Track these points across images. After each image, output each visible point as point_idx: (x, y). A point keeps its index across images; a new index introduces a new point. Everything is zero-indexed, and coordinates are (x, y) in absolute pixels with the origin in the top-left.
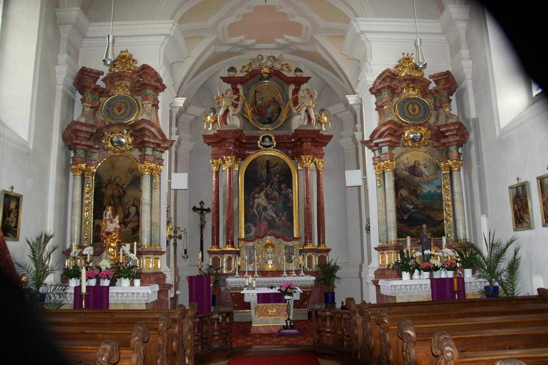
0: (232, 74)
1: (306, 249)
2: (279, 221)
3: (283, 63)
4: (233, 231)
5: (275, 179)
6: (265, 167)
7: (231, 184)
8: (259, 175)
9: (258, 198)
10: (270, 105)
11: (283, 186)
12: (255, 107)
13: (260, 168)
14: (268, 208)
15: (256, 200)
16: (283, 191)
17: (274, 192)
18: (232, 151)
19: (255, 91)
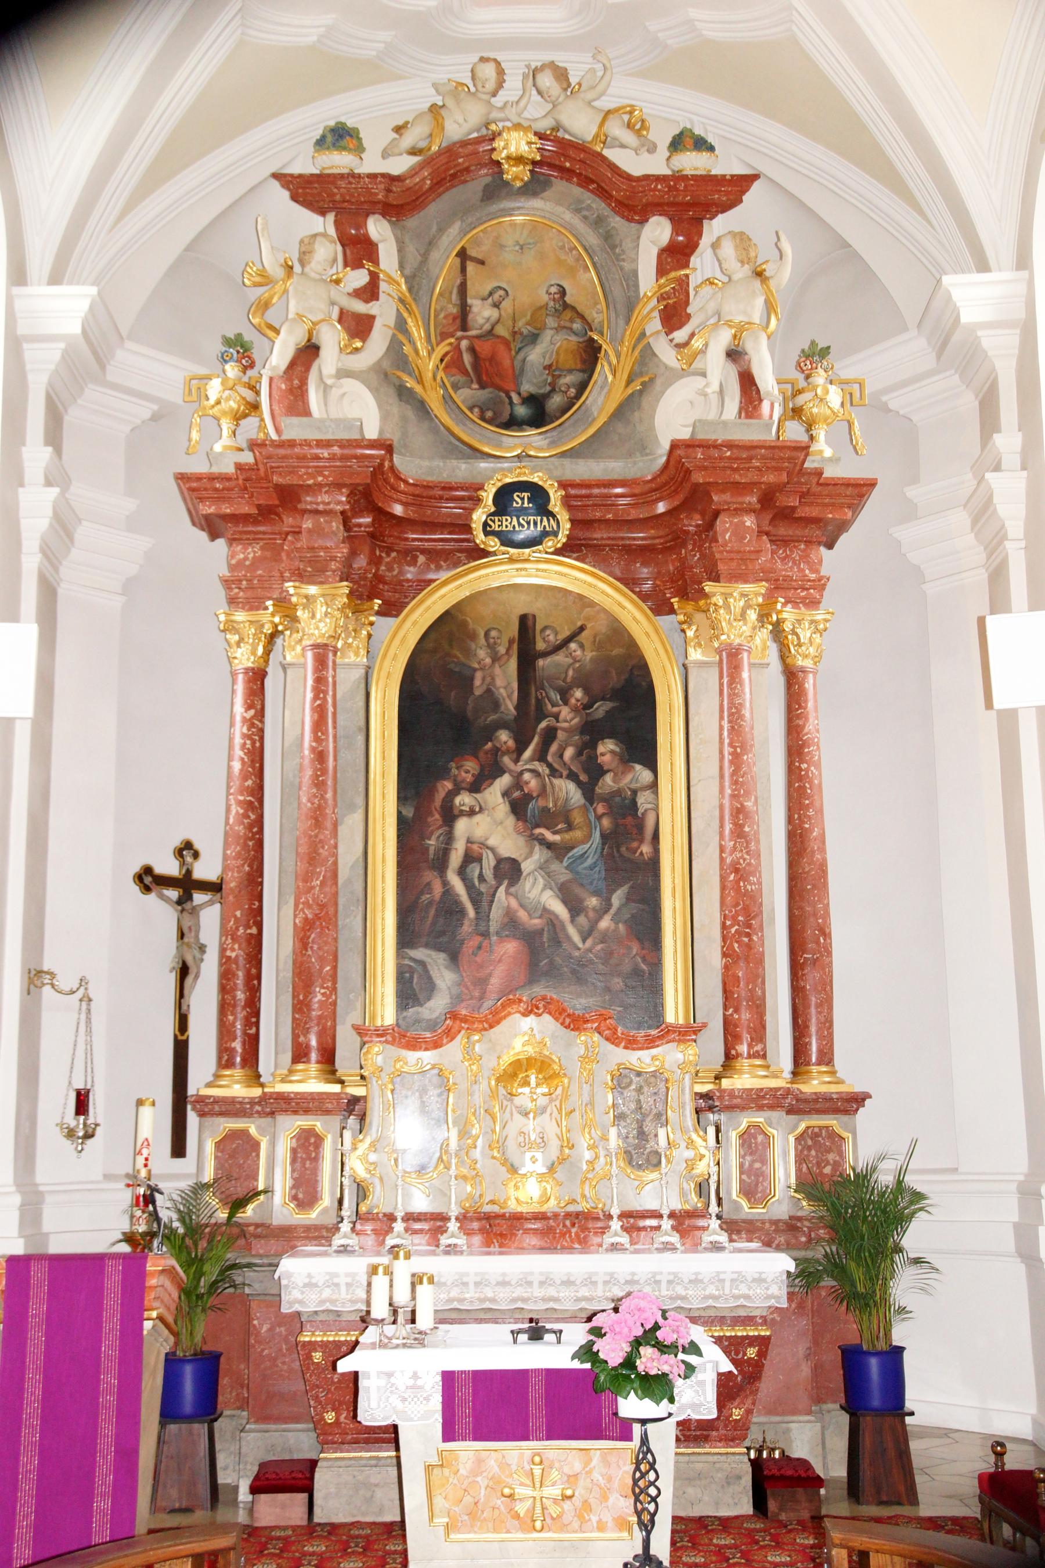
0: (339, 161)
1: (732, 1093)
2: (584, 941)
3: (607, 103)
4: (334, 989)
5: (565, 712)
7: (325, 733)
8: (478, 692)
9: (472, 813)
10: (543, 328)
11: (607, 749)
12: (459, 339)
13: (482, 653)
14: (527, 866)
15: (462, 826)
16: (608, 779)
17: (557, 782)
18: (333, 559)
19: (463, 255)
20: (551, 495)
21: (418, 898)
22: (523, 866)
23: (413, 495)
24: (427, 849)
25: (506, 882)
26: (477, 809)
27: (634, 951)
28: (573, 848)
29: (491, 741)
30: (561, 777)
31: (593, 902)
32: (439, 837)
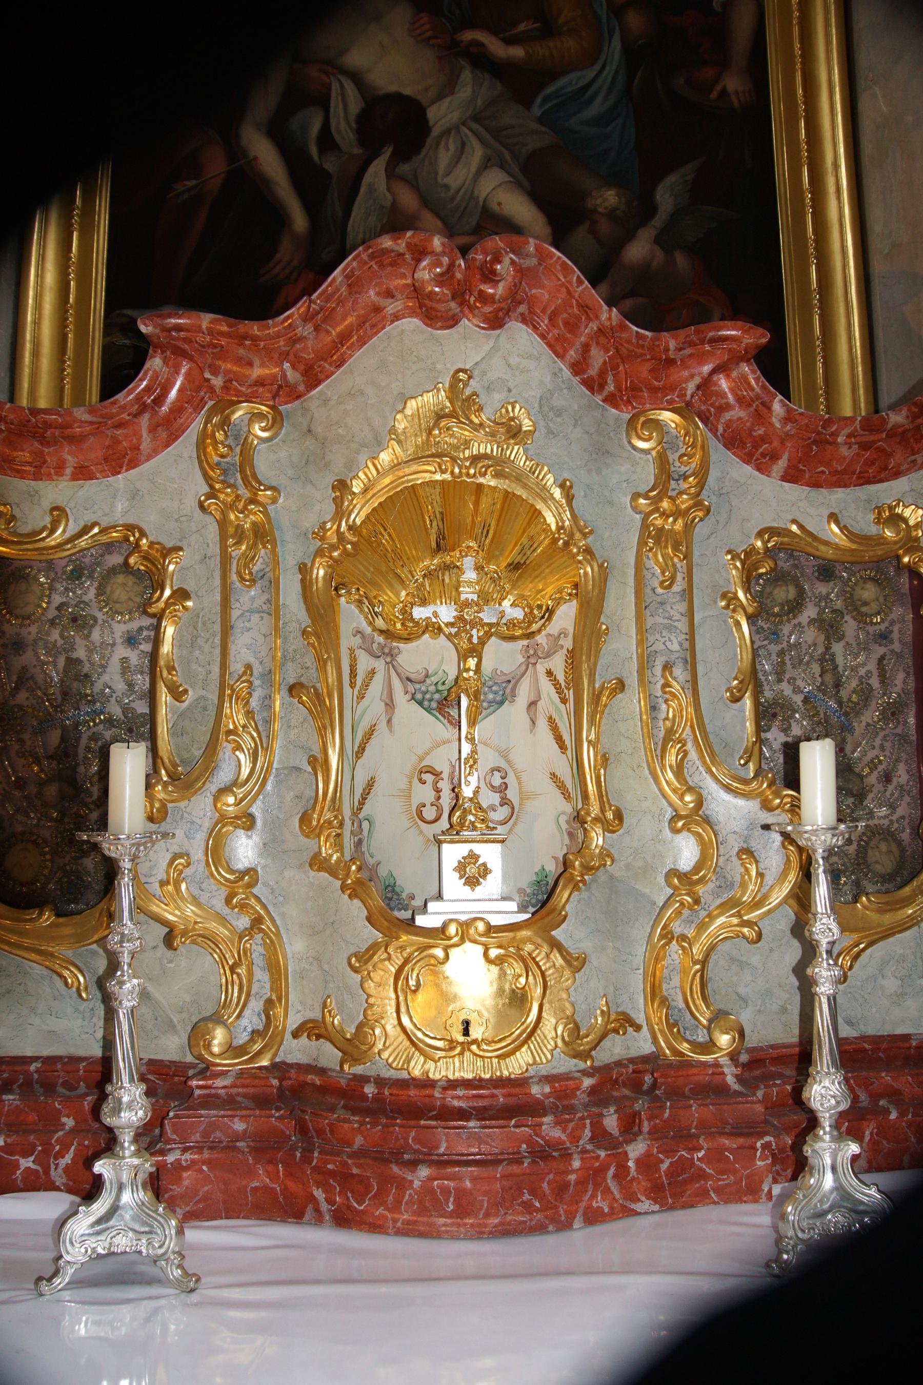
22: (432, 114)
25: (388, 152)
28: (554, 75)
31: (610, 198)
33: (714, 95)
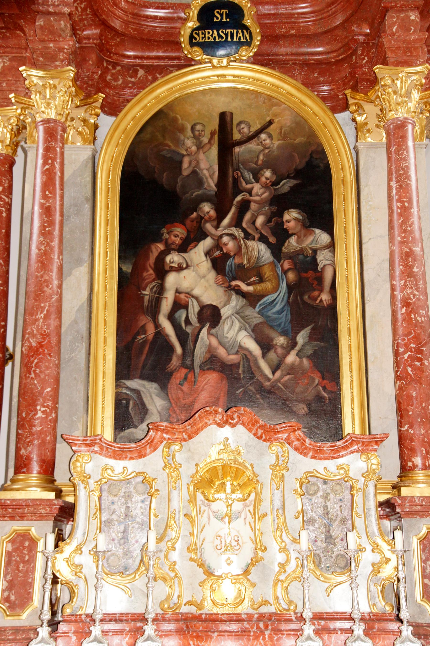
1: (412, 500)
2: (274, 373)
4: (55, 409)
6: (210, 142)
7: (53, 192)
8: (185, 173)
9: (180, 269)
13: (189, 143)
14: (225, 312)
16: (293, 241)
17: (250, 243)
20: (245, 11)
21: (135, 338)
22: (222, 311)
23: (133, 14)
24: (143, 298)
25: (208, 325)
26: (184, 266)
27: (317, 381)
28: (263, 296)
29: (196, 211)
30: (254, 239)
31: (281, 340)
32: (152, 289)
33: (318, 302)
